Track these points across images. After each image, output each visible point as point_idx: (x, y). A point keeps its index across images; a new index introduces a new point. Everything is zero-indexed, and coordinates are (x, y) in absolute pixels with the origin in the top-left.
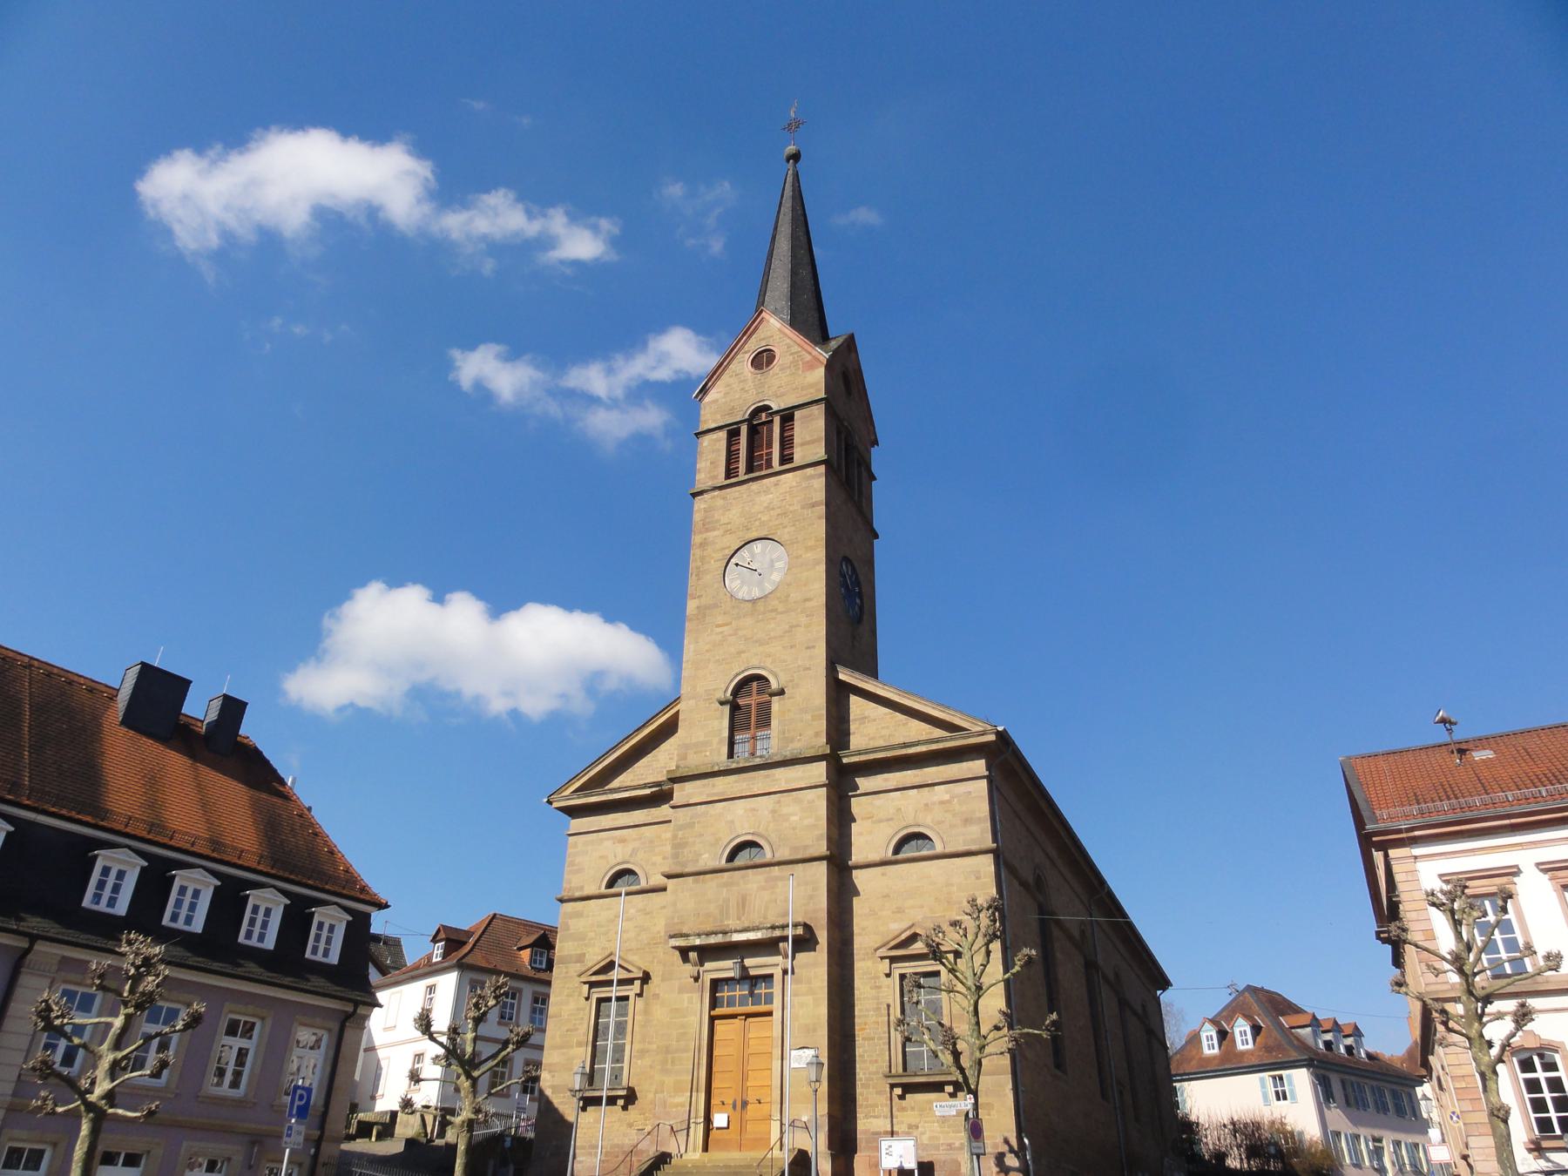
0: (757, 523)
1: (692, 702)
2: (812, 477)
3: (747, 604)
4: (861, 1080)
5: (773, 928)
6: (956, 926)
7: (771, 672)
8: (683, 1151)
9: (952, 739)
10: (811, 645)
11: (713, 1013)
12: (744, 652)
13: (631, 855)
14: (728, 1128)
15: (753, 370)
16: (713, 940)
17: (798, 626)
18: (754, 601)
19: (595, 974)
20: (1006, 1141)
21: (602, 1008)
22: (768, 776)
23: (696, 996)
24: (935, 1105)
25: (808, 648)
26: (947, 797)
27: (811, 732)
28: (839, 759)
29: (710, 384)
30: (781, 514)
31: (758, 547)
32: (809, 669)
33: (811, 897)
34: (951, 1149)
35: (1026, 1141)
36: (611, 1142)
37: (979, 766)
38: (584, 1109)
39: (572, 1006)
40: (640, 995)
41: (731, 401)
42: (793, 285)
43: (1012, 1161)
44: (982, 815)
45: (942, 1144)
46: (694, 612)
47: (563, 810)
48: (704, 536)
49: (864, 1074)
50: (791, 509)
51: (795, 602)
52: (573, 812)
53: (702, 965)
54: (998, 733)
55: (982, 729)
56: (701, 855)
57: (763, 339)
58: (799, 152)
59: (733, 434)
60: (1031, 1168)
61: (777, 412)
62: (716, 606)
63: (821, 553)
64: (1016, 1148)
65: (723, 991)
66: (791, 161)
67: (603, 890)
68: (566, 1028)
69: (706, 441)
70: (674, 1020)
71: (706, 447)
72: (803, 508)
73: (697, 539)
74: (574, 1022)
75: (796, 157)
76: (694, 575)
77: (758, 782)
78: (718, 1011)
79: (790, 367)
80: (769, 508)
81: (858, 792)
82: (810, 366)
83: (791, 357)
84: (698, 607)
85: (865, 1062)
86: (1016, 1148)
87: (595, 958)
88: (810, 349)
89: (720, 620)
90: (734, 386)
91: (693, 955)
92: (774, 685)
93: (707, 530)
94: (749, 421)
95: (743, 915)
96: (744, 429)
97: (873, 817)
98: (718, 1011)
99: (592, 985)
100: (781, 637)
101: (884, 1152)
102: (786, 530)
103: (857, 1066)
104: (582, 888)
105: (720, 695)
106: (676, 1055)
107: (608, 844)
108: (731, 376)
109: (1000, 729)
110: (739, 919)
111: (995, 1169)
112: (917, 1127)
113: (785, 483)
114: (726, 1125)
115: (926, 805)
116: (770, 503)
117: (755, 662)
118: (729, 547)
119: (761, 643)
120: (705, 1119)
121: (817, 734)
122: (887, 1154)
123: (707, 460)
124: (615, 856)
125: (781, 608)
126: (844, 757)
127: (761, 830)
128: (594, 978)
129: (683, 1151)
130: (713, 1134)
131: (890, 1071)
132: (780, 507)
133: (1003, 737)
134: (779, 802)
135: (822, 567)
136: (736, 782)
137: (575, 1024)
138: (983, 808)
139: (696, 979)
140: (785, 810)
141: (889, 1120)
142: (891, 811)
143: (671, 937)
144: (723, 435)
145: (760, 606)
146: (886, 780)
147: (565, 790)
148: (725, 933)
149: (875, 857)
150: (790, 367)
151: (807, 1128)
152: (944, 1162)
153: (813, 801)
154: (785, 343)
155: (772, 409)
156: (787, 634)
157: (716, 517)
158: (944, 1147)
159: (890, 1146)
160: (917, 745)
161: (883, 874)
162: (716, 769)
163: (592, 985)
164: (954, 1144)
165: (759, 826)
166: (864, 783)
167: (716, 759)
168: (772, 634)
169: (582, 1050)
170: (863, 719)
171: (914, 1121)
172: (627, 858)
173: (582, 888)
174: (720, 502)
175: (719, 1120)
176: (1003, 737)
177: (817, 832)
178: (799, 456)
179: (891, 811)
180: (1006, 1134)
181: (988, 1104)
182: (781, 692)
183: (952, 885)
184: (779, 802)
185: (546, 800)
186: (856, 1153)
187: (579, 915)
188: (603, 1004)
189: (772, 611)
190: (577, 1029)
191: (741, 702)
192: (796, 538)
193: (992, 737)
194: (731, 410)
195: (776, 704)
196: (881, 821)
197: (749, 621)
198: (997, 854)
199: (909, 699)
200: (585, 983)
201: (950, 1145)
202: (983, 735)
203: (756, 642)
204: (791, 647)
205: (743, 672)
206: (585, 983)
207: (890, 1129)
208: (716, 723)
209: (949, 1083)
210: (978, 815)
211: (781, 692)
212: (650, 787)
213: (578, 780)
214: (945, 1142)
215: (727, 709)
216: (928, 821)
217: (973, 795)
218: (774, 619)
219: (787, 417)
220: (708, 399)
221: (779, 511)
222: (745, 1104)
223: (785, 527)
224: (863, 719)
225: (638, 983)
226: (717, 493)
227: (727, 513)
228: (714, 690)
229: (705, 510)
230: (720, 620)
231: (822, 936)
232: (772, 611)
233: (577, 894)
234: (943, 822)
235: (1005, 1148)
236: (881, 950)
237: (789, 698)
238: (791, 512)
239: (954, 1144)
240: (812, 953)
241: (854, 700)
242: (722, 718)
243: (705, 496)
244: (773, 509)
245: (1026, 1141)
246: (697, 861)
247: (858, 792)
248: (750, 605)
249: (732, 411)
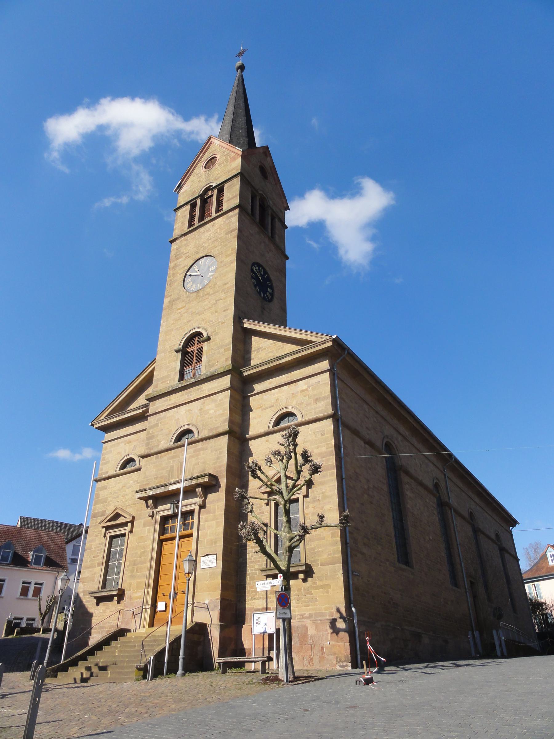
0: (202, 248)
2: (232, 216)
3: (194, 293)
4: (249, 574)
5: (192, 479)
6: (276, 455)
8: (138, 627)
9: (306, 350)
10: (225, 309)
11: (161, 537)
12: (190, 321)
13: (133, 451)
14: (165, 610)
15: (205, 170)
16: (159, 491)
17: (220, 300)
18: (197, 292)
19: (108, 521)
20: (338, 610)
21: (113, 542)
22: (198, 390)
23: (152, 528)
24: (257, 583)
25: (224, 311)
26: (305, 387)
27: (223, 359)
28: (242, 373)
29: (183, 182)
30: (215, 241)
31: (202, 262)
32: (224, 323)
33: (218, 458)
34: (303, 618)
35: (354, 610)
36: (109, 624)
37: (325, 365)
38: (98, 604)
39: (97, 542)
40: (131, 532)
41: (193, 188)
42: (233, 126)
43: (341, 624)
44: (326, 395)
45: (298, 615)
46: (167, 305)
47: (99, 428)
48: (175, 262)
49: (252, 570)
51: (219, 287)
52: (106, 429)
53: (156, 508)
54: (334, 340)
55: (323, 340)
56: (161, 441)
57: (211, 153)
58: (243, 64)
59: (193, 206)
60: (357, 629)
62: (178, 298)
63: (234, 257)
64: (345, 615)
65: (168, 524)
66: (239, 70)
67: (118, 472)
68: (93, 556)
69: (180, 212)
70: (140, 544)
71: (180, 215)
72: (226, 234)
73: (171, 265)
74: (98, 552)
75: (242, 68)
76: (168, 284)
77: (193, 393)
78: (165, 536)
79: (224, 162)
81: (254, 393)
82: (234, 159)
83: (225, 157)
84: (169, 302)
85: (252, 562)
86: (345, 615)
87: (109, 511)
91: (150, 502)
93: (177, 259)
94: (201, 196)
96: (199, 201)
97: (262, 407)
98: (165, 536)
99: (107, 528)
101: (255, 622)
102: (217, 249)
103: (247, 565)
104: (107, 472)
105: (177, 347)
106: (139, 566)
109: (334, 337)
111: (330, 631)
113: (218, 223)
114: (164, 609)
115: (293, 394)
116: (209, 237)
117: (196, 325)
119: (200, 313)
120: (152, 605)
121: (227, 360)
122: (257, 623)
123: (179, 223)
124: (125, 452)
125: (211, 292)
126: (244, 372)
127: (193, 422)
128: (108, 524)
129: (138, 627)
130: (158, 615)
131: (267, 567)
133: (337, 342)
134: (204, 403)
135: (234, 265)
136: (181, 396)
137: (98, 553)
138: (327, 390)
139: (152, 516)
140: (207, 408)
141: (265, 600)
142: (272, 402)
143: (137, 492)
144: (188, 207)
145: (201, 294)
146: (270, 383)
147: (101, 416)
148: (165, 486)
149: (262, 430)
150: (224, 162)
151: (208, 608)
152: (298, 627)
153: (222, 399)
154: (222, 151)
155: (213, 186)
156: (213, 306)
157: (182, 251)
158: (299, 617)
159: (259, 618)
160: (286, 357)
161: (267, 441)
162: (170, 389)
163: (107, 528)
164: (305, 614)
165: (192, 420)
166: (258, 387)
168: (206, 308)
169: (100, 568)
170: (259, 349)
172: (130, 452)
173: (107, 472)
174: (184, 242)
175: (161, 606)
176: (337, 342)
177: (224, 418)
178: (225, 207)
179: (272, 402)
180: (338, 606)
181: (327, 585)
183: (307, 441)
184: (204, 403)
185: (90, 424)
186: (244, 624)
187: (104, 488)
188: (114, 540)
189: (207, 294)
190: (98, 556)
191: (189, 350)
192: (222, 252)
193: (330, 344)
194: (193, 193)
195: (205, 346)
196: (267, 408)
198: (334, 417)
199: (282, 330)
200: (103, 527)
201: (302, 615)
202: (324, 343)
203: (198, 313)
204: (216, 312)
205: (189, 332)
206: (103, 527)
207: (265, 607)
209: (300, 572)
210: (323, 395)
211: (209, 339)
212: (142, 408)
213: (107, 410)
214: (300, 613)
215: (180, 354)
216: (294, 403)
217: (321, 383)
219: (220, 189)
220: (182, 191)
223: (216, 247)
224: (259, 349)
225: (130, 524)
226: (183, 238)
227: (187, 247)
228: (174, 345)
229: (177, 249)
231: (223, 482)
232: (207, 294)
233: (104, 476)
234: (303, 403)
235: (338, 615)
236: (262, 488)
237: (213, 342)
238: (220, 238)
239: (305, 614)
240: (217, 493)
241: (255, 341)
242: (177, 360)
243: (178, 241)
245: (354, 610)
246: (158, 445)
247: (254, 393)
248: (195, 294)
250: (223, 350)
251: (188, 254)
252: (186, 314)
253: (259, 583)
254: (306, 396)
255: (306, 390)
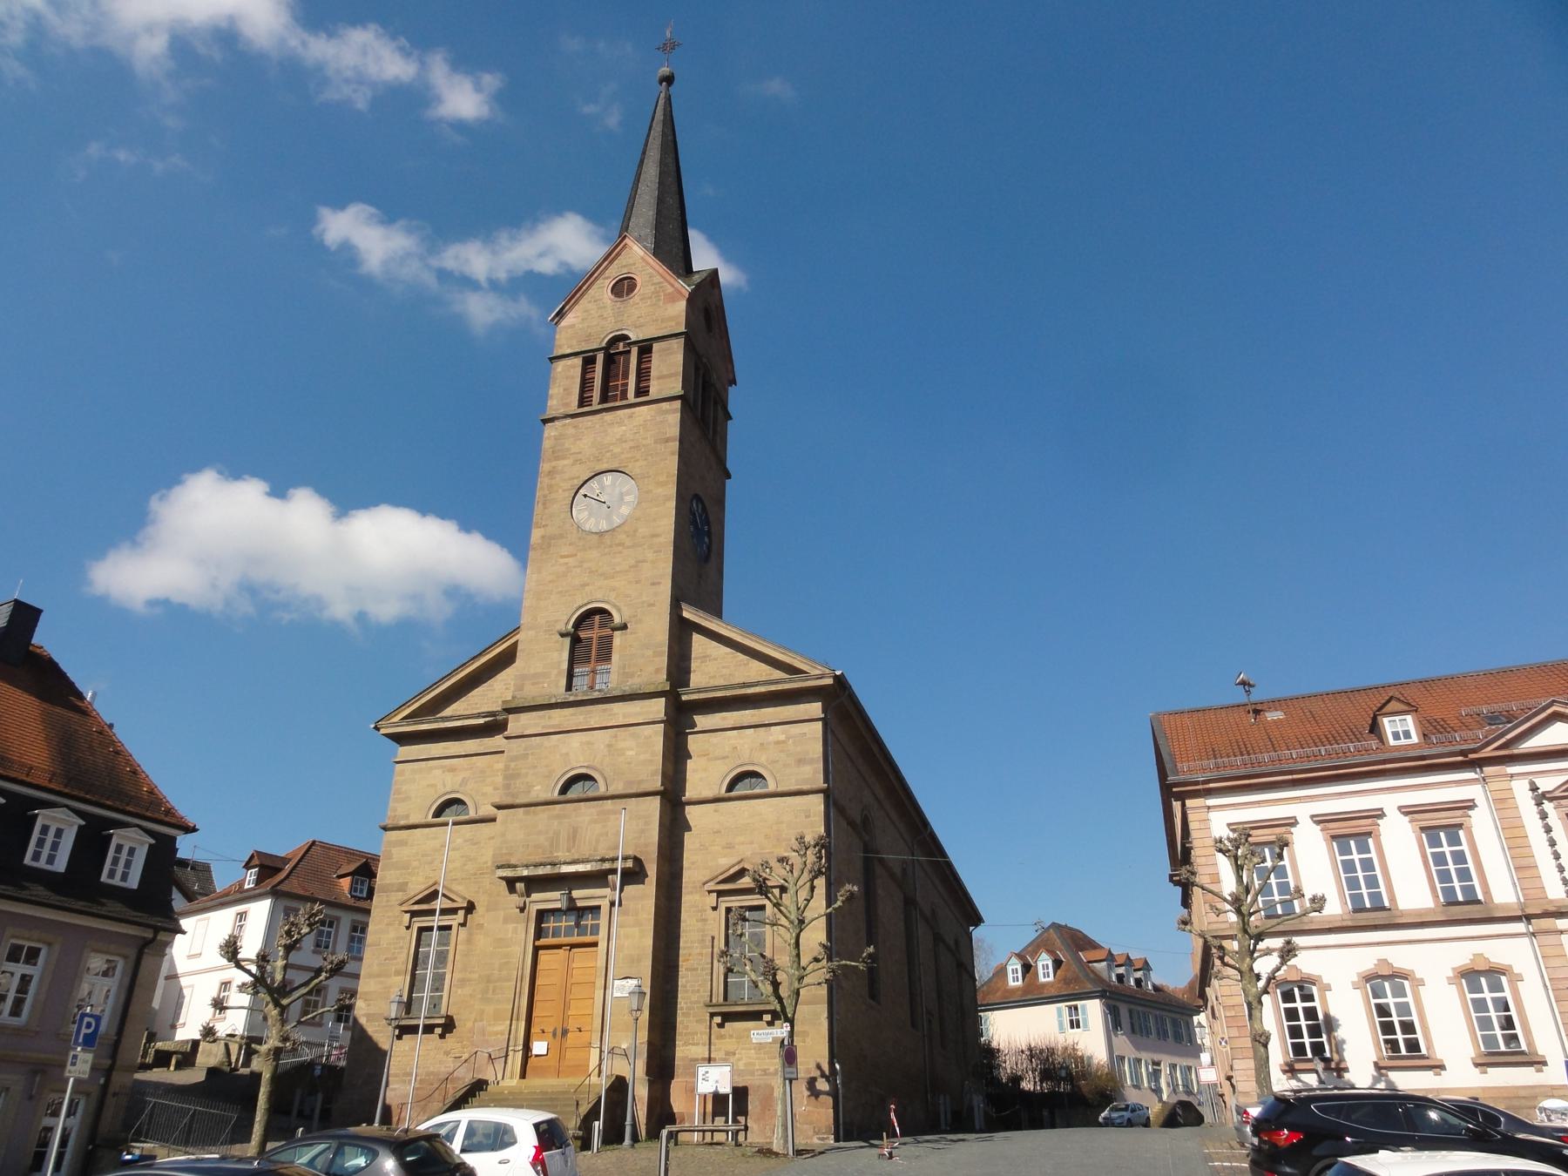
0: (609, 454)
1: (532, 633)
2: (667, 412)
3: (594, 536)
4: (682, 1008)
5: (603, 860)
6: (783, 862)
7: (615, 606)
8: (500, 1077)
9: (791, 681)
10: (655, 581)
11: (537, 943)
12: (588, 585)
13: (460, 785)
14: (547, 1055)
15: (612, 297)
16: (541, 871)
17: (644, 561)
18: (601, 534)
19: (417, 903)
20: (819, 1067)
21: (423, 938)
22: (605, 710)
23: (521, 927)
24: (752, 1032)
25: (653, 584)
26: (782, 737)
27: (651, 669)
28: (679, 695)
29: (567, 307)
30: (634, 447)
31: (608, 479)
32: (653, 605)
33: (643, 831)
34: (766, 1074)
35: (838, 1066)
37: (815, 709)
38: (399, 1037)
39: (392, 935)
40: (463, 925)
41: (588, 327)
42: (659, 213)
43: (822, 1085)
44: (816, 756)
45: (757, 1070)
46: (540, 541)
47: (391, 736)
48: (554, 464)
49: (686, 1003)
50: (644, 442)
51: (643, 538)
52: (401, 739)
53: (529, 896)
54: (836, 678)
55: (820, 672)
56: (534, 786)
57: (625, 266)
58: (673, 74)
59: (589, 361)
60: (840, 1091)
61: (635, 343)
62: (561, 536)
63: (671, 490)
64: (827, 1073)
65: (548, 922)
66: (664, 83)
67: (430, 819)
68: (385, 957)
69: (560, 366)
70: (497, 950)
71: (560, 373)
72: (656, 442)
73: (545, 467)
74: (393, 951)
75: (669, 80)
76: (540, 505)
77: (596, 715)
78: (543, 942)
79: (651, 297)
80: (622, 440)
81: (696, 730)
82: (672, 299)
83: (653, 287)
84: (543, 537)
85: (687, 991)
86: (827, 1073)
87: (418, 887)
88: (672, 281)
89: (565, 550)
90: (592, 312)
91: (520, 886)
92: (617, 620)
93: (557, 458)
94: (606, 349)
95: (574, 846)
96: (600, 357)
97: (708, 754)
98: (543, 942)
99: (414, 914)
100: (626, 571)
101: (700, 1077)
102: (638, 464)
103: (679, 996)
104: (407, 817)
105: (561, 627)
106: (498, 984)
107: (437, 772)
108: (590, 302)
109: (838, 673)
110: (569, 851)
111: (807, 1093)
112: (734, 1054)
113: (639, 416)
114: (545, 1053)
115: (762, 744)
116: (622, 435)
117: (599, 596)
118: (578, 477)
119: (604, 576)
120: (524, 1046)
121: (657, 671)
122: (703, 1079)
123: (559, 386)
124: (444, 786)
125: (628, 543)
126: (684, 694)
128: (416, 907)
129: (500, 1077)
130: (531, 1061)
131: (711, 1001)
132: (633, 440)
133: (840, 681)
134: (616, 736)
135: (673, 504)
136: (572, 715)
137: (394, 953)
138: (817, 749)
139: (522, 910)
140: (621, 745)
141: (707, 1047)
142: (727, 750)
143: (499, 867)
144: (578, 361)
145: (607, 539)
146: (724, 719)
147: (395, 715)
148: (554, 864)
149: (708, 793)
150: (651, 297)
151: (626, 1055)
152: (759, 1087)
153: (650, 736)
154: (648, 272)
155: (630, 339)
156: (632, 569)
157: (567, 445)
158: (760, 1072)
159: (707, 1072)
160: (756, 686)
161: (716, 811)
162: (553, 701)
163: (414, 914)
164: (768, 1069)
165: (594, 761)
166: (702, 721)
167: (554, 691)
168: (618, 569)
169: (401, 978)
170: (705, 658)
171: (730, 1048)
172: (456, 788)
173: (407, 817)
174: (571, 431)
175: (539, 1047)
176: (840, 681)
177: (654, 768)
178: (654, 391)
179: (727, 750)
180: (819, 1060)
181: (804, 1032)
182: (624, 627)
183: (782, 822)
184: (616, 736)
185: (373, 726)
186: (673, 1078)
187: (403, 843)
188: (424, 933)
189: (619, 545)
190: (395, 958)
191: (582, 635)
192: (648, 473)
193: (830, 681)
195: (618, 638)
196: (717, 758)
197: (594, 554)
198: (826, 793)
199: (751, 639)
200: (406, 912)
201: (765, 1071)
202: (821, 678)
203: (601, 575)
204: (637, 582)
205: (586, 605)
206: (406, 912)
207: (707, 1056)
208: (556, 655)
209: (767, 1012)
211: (624, 627)
212: (484, 717)
213: (409, 706)
214: (762, 1068)
215: (567, 641)
216: (763, 759)
217: (808, 736)
218: (620, 552)
219: (645, 348)
220: (563, 323)
221: (632, 444)
222: (565, 1032)
223: (637, 460)
224: (705, 658)
225: (461, 913)
226: (568, 421)
227: (578, 442)
228: (556, 621)
229: (556, 438)
230: (565, 550)
231: (652, 870)
232: (619, 545)
233: (402, 823)
234: (778, 761)
235: (817, 1073)
236: (709, 884)
238: (644, 445)
239: (768, 1069)
240: (641, 886)
241: (698, 640)
242: (562, 650)
243: (557, 423)
244: (626, 441)
245: (838, 1066)
246: (529, 792)
247: (696, 730)
248: (596, 537)
249: (588, 338)
250: (650, 653)
251: (579, 456)
252: (578, 570)
253: (756, 1032)
254: (782, 751)
255: (783, 742)
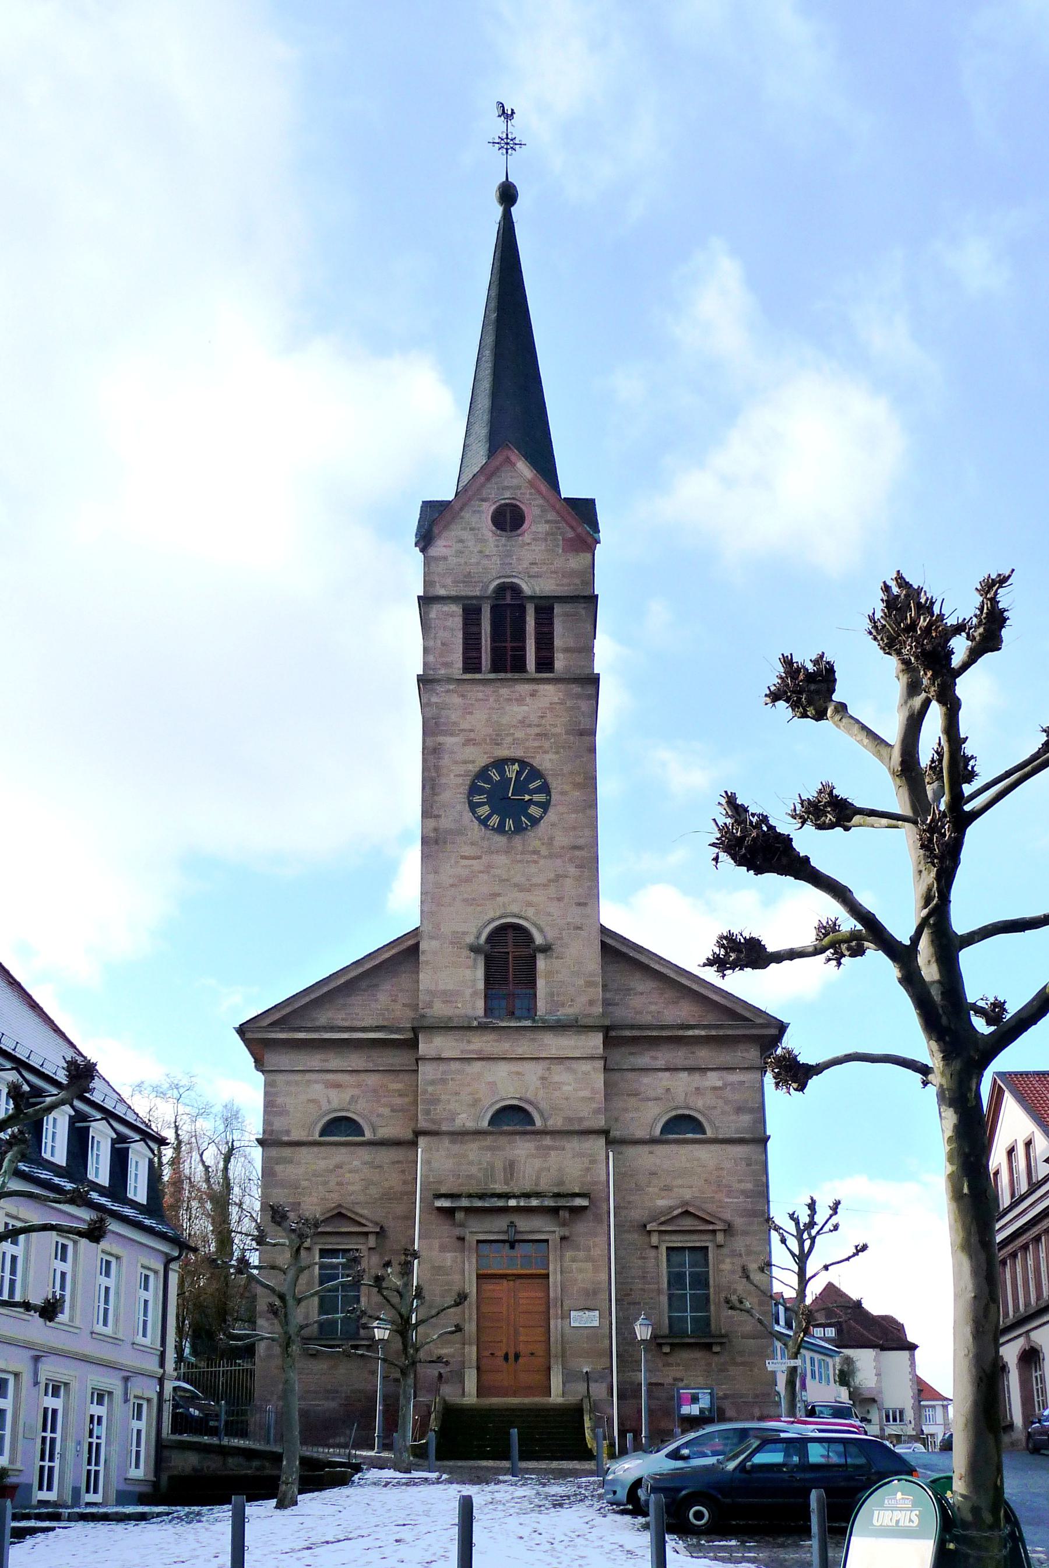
1: (435, 944)
7: (535, 925)
12: (499, 895)
13: (349, 1103)
25: (579, 904)
26: (719, 1084)
27: (583, 999)
33: (588, 1169)
36: (351, 1388)
50: (554, 730)
61: (532, 598)
67: (316, 1137)
80: (524, 723)
88: (574, 524)
89: (468, 850)
90: (470, 544)
92: (539, 940)
95: (512, 1179)
100: (544, 886)
102: (548, 757)
107: (319, 1087)
108: (465, 529)
110: (507, 1183)
112: (682, 1381)
115: (697, 1089)
117: (515, 908)
118: (473, 762)
127: (530, 1095)
132: (538, 726)
134: (549, 1069)
140: (556, 1078)
161: (651, 1153)
167: (470, 1012)
168: (534, 880)
171: (678, 1375)
173: (288, 1132)
182: (546, 949)
194: (465, 576)
195: (541, 963)
196: (649, 1100)
197: (502, 860)
208: (468, 972)
210: (750, 1105)
216: (700, 1104)
218: (536, 862)
221: (537, 730)
222: (517, 1356)
223: (545, 752)
228: (464, 933)
230: (468, 850)
237: (557, 958)
244: (530, 726)
249: (467, 579)
250: (581, 982)
251: (472, 735)
252: (485, 877)
254: (721, 1098)
255: (720, 1088)
